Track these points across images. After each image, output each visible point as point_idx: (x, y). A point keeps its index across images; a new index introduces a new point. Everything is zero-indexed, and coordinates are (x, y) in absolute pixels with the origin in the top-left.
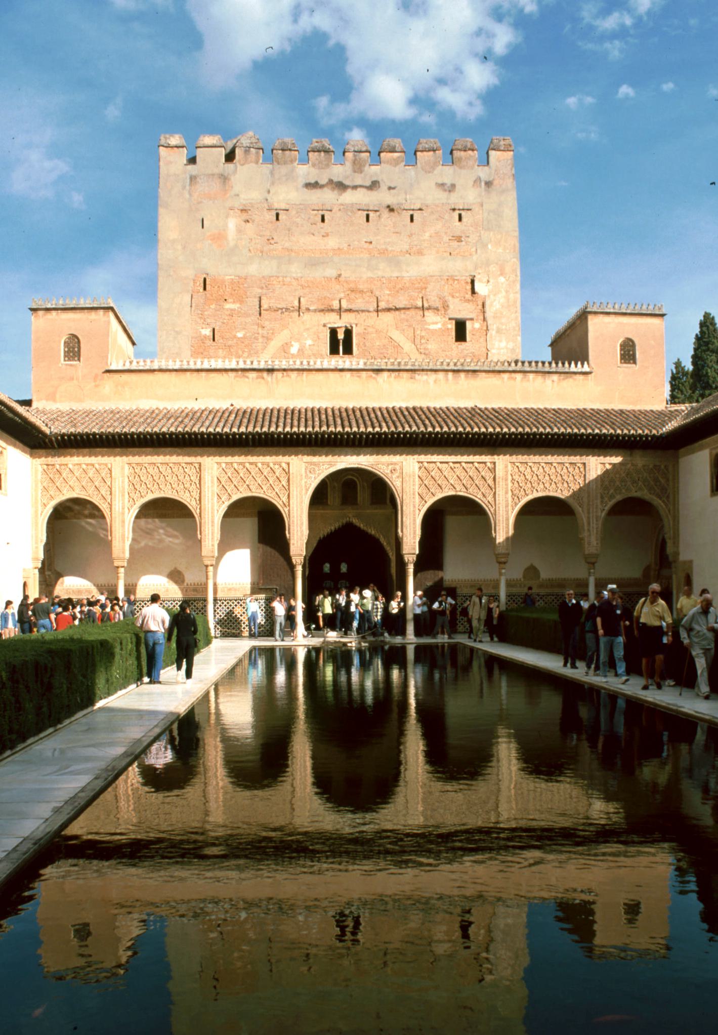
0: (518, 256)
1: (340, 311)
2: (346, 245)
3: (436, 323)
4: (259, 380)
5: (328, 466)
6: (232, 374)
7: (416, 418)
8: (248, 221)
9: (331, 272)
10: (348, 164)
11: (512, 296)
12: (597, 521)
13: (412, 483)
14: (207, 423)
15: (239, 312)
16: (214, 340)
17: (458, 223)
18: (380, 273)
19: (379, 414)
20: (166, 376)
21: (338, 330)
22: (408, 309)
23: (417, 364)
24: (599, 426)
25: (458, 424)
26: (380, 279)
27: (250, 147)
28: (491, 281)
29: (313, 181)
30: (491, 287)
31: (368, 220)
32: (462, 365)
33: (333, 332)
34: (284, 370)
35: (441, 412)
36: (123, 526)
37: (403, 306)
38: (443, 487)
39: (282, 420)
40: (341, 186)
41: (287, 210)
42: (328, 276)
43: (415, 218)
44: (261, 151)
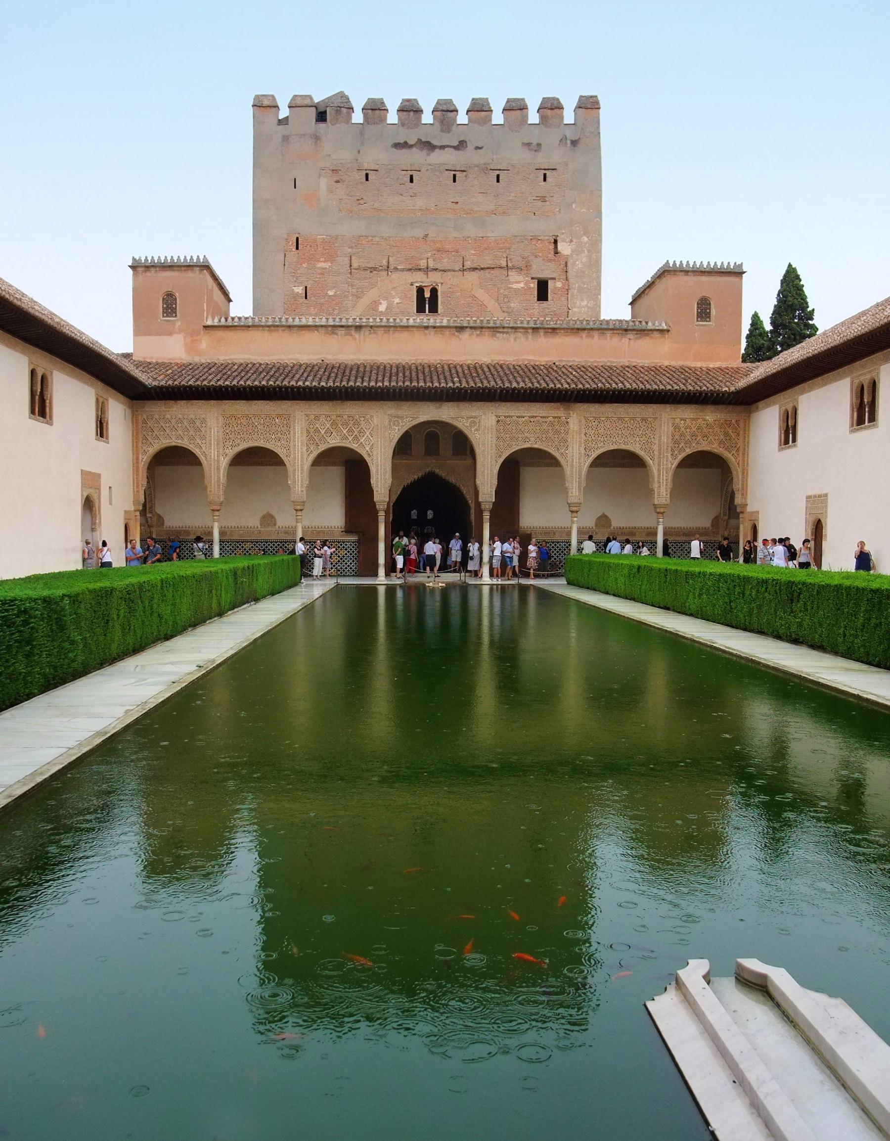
1: (427, 270)
3: (519, 282)
6: (322, 330)
9: (419, 232)
13: (490, 436)
14: (297, 376)
16: (306, 298)
17: (543, 183)
21: (425, 288)
22: (493, 268)
23: (498, 322)
24: (671, 382)
25: (534, 380)
27: (341, 107)
29: (402, 142)
31: (454, 181)
33: (420, 291)
34: (371, 327)
35: (519, 369)
36: (219, 473)
38: (520, 439)
39: (367, 375)
40: (428, 146)
43: (500, 178)
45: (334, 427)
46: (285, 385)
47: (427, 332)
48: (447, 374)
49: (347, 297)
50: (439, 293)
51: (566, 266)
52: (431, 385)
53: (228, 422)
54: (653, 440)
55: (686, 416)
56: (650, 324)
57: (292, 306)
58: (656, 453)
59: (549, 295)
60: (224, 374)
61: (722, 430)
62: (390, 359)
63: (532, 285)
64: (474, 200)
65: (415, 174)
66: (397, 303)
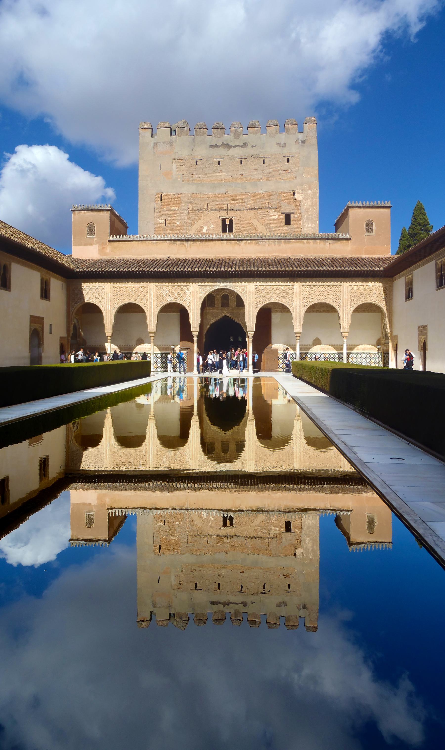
1: (227, 210)
4: (181, 245)
6: (169, 242)
9: (223, 190)
10: (232, 134)
12: (347, 315)
13: (252, 296)
14: (152, 266)
16: (166, 226)
17: (287, 163)
19: (238, 261)
20: (137, 243)
29: (214, 145)
30: (304, 196)
31: (241, 164)
32: (283, 237)
33: (224, 221)
34: (194, 240)
39: (188, 265)
44: (189, 129)
45: (170, 292)
46: (144, 270)
47: (222, 242)
48: (231, 264)
50: (233, 222)
52: (220, 269)
53: (116, 290)
54: (339, 297)
55: (357, 283)
57: (158, 230)
58: (341, 304)
60: (114, 265)
61: (378, 291)
62: (203, 256)
63: (282, 217)
64: (252, 173)
66: (212, 228)
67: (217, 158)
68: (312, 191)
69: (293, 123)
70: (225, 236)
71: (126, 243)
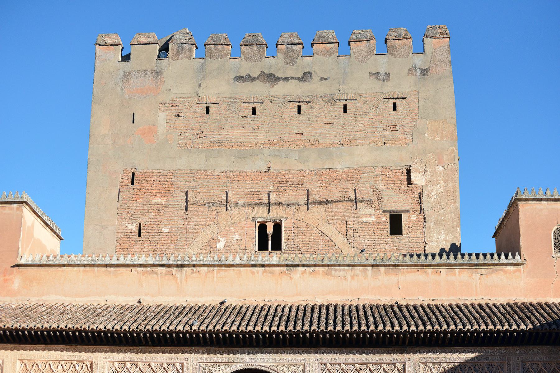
0: (456, 143)
2: (277, 137)
3: (370, 216)
5: (224, 367)
7: (324, 316)
8: (179, 116)
9: (261, 165)
10: (280, 56)
11: (451, 185)
15: (166, 207)
16: (140, 235)
18: (311, 166)
20: (75, 270)
21: (267, 224)
22: (341, 201)
23: (334, 259)
24: (519, 321)
26: (310, 171)
28: (428, 170)
29: (244, 75)
30: (428, 177)
31: (299, 112)
33: (262, 227)
34: (194, 266)
37: (336, 199)
39: (178, 319)
41: (218, 104)
42: (257, 168)
47: (254, 270)
49: (183, 235)
51: (420, 198)
56: (503, 257)
59: (403, 228)
63: (384, 219)
64: (320, 131)
65: (258, 106)
66: (237, 240)
67: (249, 101)
68: (446, 166)
69: (403, 36)
70: (260, 258)
71: (53, 270)
